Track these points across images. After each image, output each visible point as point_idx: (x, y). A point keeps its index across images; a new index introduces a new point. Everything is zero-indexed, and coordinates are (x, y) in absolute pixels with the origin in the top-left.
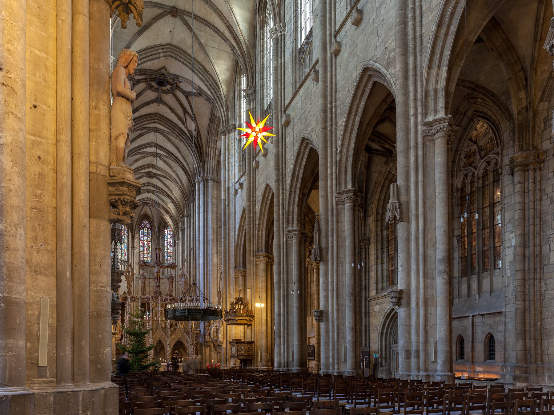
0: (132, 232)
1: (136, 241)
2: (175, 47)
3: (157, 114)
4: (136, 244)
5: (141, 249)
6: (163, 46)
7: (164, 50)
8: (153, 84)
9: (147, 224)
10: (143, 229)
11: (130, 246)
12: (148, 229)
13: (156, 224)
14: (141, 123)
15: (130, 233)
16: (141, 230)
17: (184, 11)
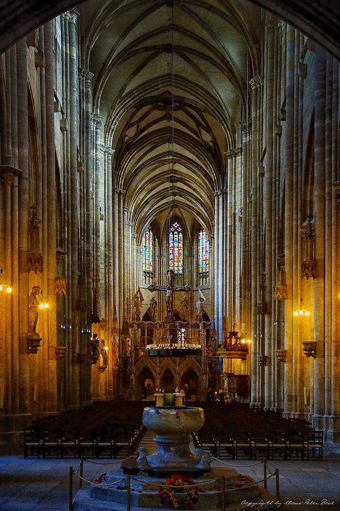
1: (164, 247)
2: (175, 76)
3: (169, 127)
4: (164, 253)
5: (171, 256)
6: (162, 77)
7: (163, 81)
8: (159, 104)
10: (173, 234)
11: (157, 254)
13: (189, 227)
14: (151, 139)
16: (171, 235)
17: (180, 46)
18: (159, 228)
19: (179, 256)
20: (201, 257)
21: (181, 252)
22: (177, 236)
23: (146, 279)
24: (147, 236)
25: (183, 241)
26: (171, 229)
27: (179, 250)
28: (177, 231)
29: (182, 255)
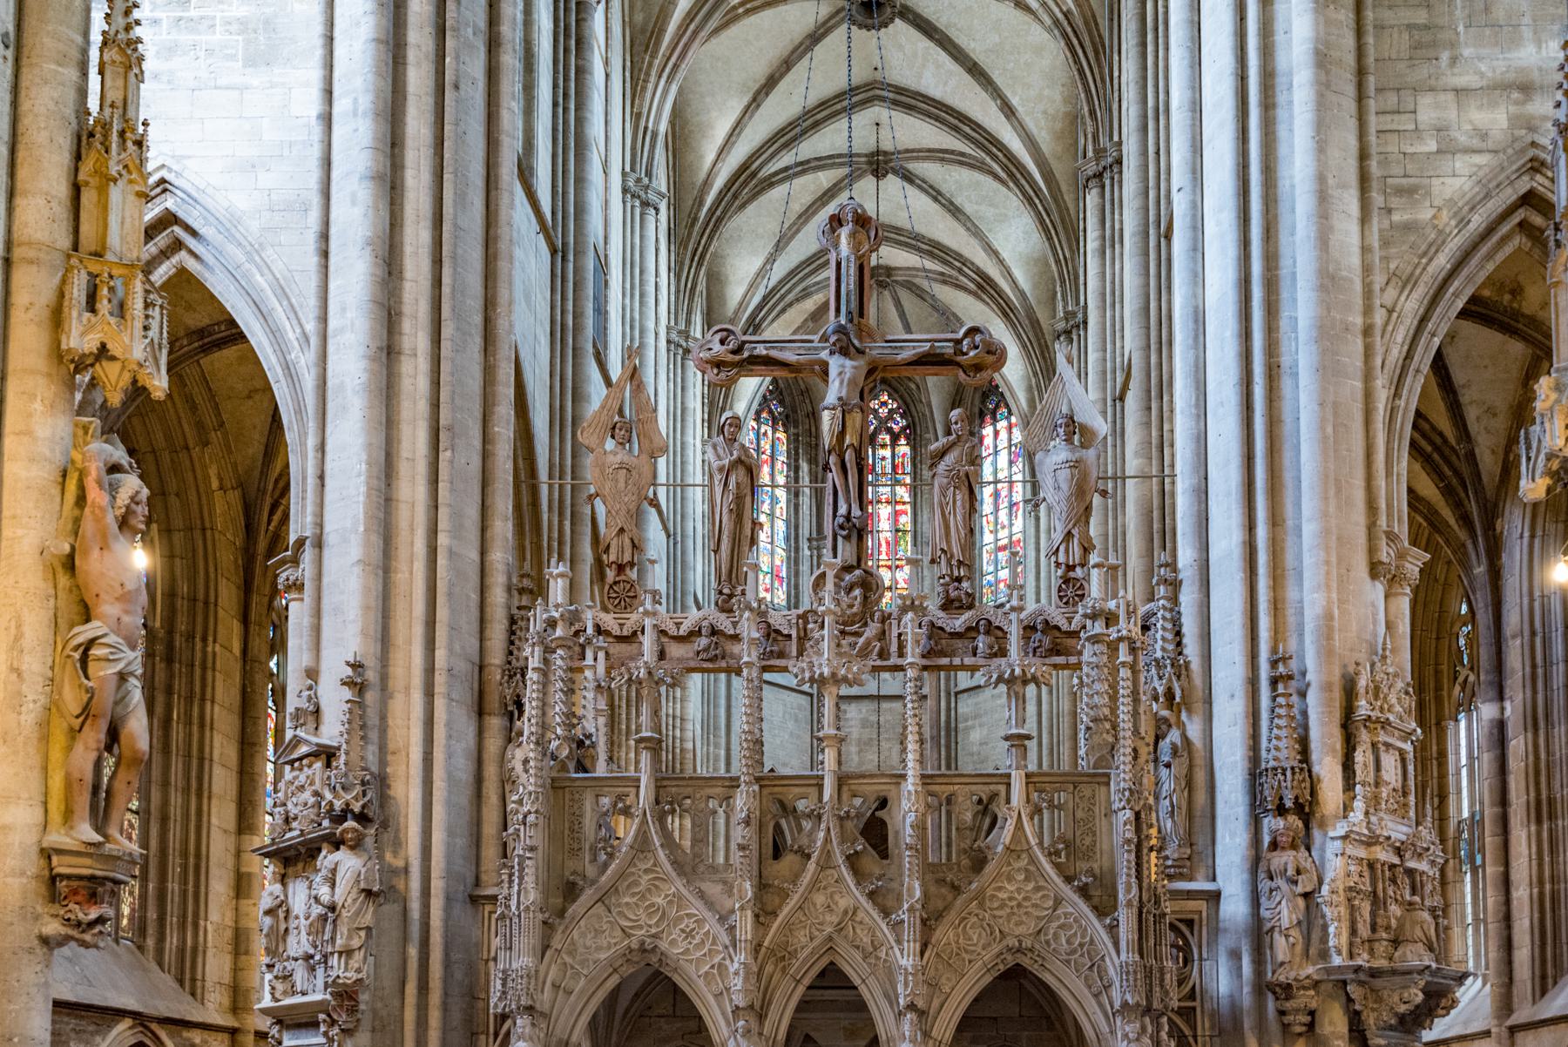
0: (812, 461)
9: (890, 416)
11: (805, 531)
12: (895, 439)
15: (804, 466)
19: (897, 542)
20: (988, 538)
21: (906, 520)
22: (887, 453)
25: (915, 474)
27: (897, 514)
28: (889, 430)
29: (909, 538)
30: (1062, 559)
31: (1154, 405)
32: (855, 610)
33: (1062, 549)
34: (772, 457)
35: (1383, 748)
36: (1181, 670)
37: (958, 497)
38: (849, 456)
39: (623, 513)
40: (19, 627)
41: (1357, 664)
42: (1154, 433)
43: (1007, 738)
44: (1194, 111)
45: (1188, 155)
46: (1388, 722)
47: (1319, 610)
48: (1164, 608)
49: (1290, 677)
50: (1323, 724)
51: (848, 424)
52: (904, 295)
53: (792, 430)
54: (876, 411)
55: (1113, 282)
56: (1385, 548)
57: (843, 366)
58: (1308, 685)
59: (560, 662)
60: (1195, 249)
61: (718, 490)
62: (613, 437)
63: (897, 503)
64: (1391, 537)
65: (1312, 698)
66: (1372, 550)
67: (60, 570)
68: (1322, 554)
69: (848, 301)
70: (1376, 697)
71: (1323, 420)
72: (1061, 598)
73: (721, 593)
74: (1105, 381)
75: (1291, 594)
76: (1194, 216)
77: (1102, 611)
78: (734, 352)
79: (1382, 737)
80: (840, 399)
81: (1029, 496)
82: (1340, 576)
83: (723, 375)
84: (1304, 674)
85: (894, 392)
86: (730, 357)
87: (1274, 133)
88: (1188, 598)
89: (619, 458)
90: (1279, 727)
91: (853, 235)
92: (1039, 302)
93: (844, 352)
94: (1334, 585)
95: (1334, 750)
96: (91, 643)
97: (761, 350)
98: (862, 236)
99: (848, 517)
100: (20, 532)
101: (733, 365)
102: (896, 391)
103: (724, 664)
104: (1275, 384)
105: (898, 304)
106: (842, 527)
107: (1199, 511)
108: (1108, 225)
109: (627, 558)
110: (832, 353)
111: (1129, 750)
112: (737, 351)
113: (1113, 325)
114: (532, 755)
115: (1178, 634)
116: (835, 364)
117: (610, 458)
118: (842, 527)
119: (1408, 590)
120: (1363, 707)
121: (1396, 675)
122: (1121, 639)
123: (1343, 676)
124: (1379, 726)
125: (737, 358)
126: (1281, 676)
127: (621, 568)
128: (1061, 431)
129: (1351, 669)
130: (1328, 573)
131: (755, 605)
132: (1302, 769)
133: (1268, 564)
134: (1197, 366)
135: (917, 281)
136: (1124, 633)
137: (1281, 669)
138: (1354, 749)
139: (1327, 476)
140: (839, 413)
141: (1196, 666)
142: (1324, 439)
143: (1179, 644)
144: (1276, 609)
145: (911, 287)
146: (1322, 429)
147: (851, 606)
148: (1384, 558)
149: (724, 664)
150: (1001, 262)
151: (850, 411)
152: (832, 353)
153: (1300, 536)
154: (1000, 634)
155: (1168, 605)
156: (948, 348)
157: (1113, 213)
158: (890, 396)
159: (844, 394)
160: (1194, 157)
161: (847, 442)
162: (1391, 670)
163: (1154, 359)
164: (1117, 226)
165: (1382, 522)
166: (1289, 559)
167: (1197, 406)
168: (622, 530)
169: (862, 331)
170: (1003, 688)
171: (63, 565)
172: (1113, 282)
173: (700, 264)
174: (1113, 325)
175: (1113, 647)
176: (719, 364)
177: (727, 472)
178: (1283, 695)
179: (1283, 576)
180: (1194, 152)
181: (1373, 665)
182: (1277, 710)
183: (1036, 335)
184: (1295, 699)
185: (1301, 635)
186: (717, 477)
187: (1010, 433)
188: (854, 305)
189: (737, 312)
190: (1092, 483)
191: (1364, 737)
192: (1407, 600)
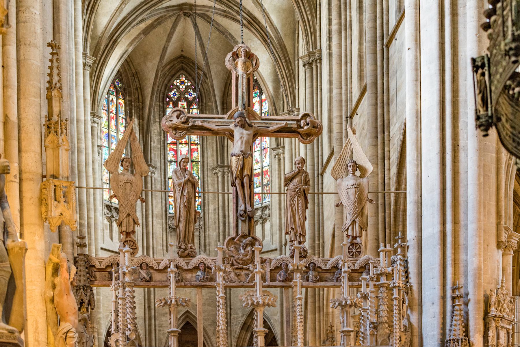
0: (141, 117)
10: (175, 105)
12: (190, 104)
18: (140, 89)
23: (111, 226)
24: (113, 108)
26: (171, 94)
27: (192, 151)
28: (186, 99)
30: (350, 233)
31: (379, 137)
32: (248, 257)
33: (350, 228)
34: (117, 114)
35: (500, 328)
36: (408, 290)
37: (300, 202)
38: (246, 180)
39: (129, 206)
40: (37, 324)
41: (491, 291)
42: (380, 151)
43: (342, 332)
44: (416, 9)
45: (413, 32)
46: (503, 317)
47: (475, 266)
48: (401, 260)
49: (461, 297)
50: (476, 319)
51: (246, 164)
52: (200, 21)
53: (128, 98)
54: (178, 87)
55: (346, 50)
56: (504, 234)
57: (242, 134)
58: (469, 300)
59: (128, 294)
60: (417, 80)
61: (178, 195)
62: (122, 165)
63: (192, 144)
64: (507, 229)
65: (471, 306)
66: (498, 236)
67: (48, 302)
68: (477, 239)
69: (243, 98)
70: (499, 305)
71: (479, 175)
72: (349, 253)
73: (180, 248)
74: (341, 106)
75: (462, 257)
76: (416, 63)
77: (385, 273)
78: (183, 123)
79: (501, 324)
80: (242, 151)
81: (274, 146)
82: (484, 248)
83: (178, 135)
84: (467, 295)
85: (190, 76)
86: (183, 126)
87: (457, 28)
88: (412, 255)
89: (126, 177)
90: (456, 320)
91: (244, 63)
92: (285, 35)
93: (243, 126)
94: (482, 254)
95: (480, 331)
96: (68, 332)
97: (198, 122)
98: (249, 63)
99: (245, 211)
100: (34, 287)
101: (184, 129)
102: (190, 75)
103: (183, 284)
104: (456, 154)
105: (195, 26)
106: (241, 216)
107: (418, 212)
108: (343, 17)
109: (131, 229)
110: (236, 126)
111: (398, 337)
112: (186, 122)
113: (346, 75)
114: (120, 339)
115: (407, 272)
116: (238, 132)
117: (121, 177)
118: (241, 216)
119: (512, 253)
120: (493, 311)
121: (507, 294)
122: (395, 287)
123: (484, 296)
124: (499, 319)
125: (186, 126)
126: (458, 296)
127: (128, 234)
128: (350, 169)
129: (488, 292)
130: (480, 248)
131: (223, 268)
132: (465, 340)
133: (450, 241)
134: (417, 140)
135: (209, 14)
136: (397, 284)
137: (457, 293)
138: (488, 330)
139: (480, 202)
140: (241, 158)
141: (415, 288)
142: (480, 184)
143: (407, 277)
144: (455, 263)
145: (208, 19)
146: (479, 179)
147: (246, 256)
148: (504, 240)
149: (183, 284)
150: (264, 11)
151: (247, 157)
152: (236, 126)
153: (467, 229)
154: (320, 270)
155: (403, 259)
156: (294, 125)
157: (346, 11)
158: (186, 78)
159: (243, 149)
160: (416, 33)
161: (245, 173)
162: (505, 292)
163: (379, 111)
164: (348, 19)
165: (503, 222)
166: (462, 241)
167: (417, 160)
168: (129, 215)
169: (252, 114)
170: (340, 308)
171: (50, 300)
172: (346, 50)
173: (92, 12)
174: (346, 75)
175: (390, 290)
176: (176, 129)
177: (183, 186)
178: (458, 305)
179: (458, 248)
180: (416, 30)
181: (497, 291)
182: (455, 312)
183: (284, 55)
184: (463, 307)
185: (466, 276)
186: (177, 189)
187: (261, 105)
188: (246, 100)
189: (103, 33)
190: (365, 196)
191: (493, 324)
192: (511, 257)
